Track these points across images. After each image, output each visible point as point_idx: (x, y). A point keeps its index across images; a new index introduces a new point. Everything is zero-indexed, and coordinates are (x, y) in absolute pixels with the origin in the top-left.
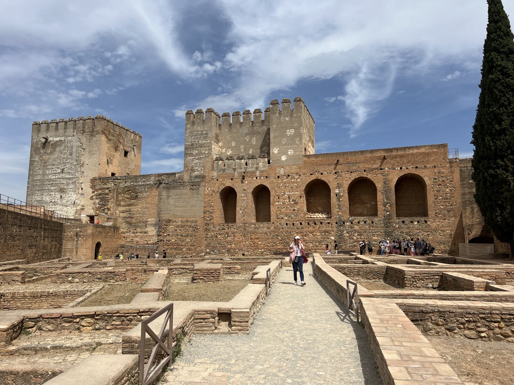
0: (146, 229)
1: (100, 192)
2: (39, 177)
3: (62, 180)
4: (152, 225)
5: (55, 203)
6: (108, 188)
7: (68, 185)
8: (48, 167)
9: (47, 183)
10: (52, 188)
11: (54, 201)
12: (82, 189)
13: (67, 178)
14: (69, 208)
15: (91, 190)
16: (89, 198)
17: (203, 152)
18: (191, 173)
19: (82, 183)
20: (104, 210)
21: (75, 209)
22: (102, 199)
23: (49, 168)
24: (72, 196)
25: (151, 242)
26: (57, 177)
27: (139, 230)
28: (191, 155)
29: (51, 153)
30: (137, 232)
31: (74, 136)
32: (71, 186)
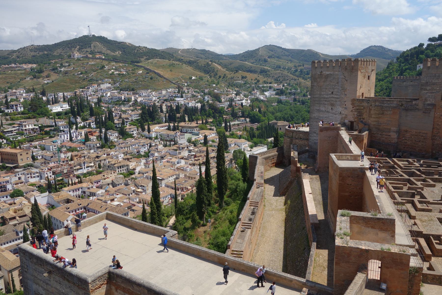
0: (390, 134)
1: (357, 108)
2: (317, 96)
3: (332, 99)
4: (394, 132)
5: (328, 112)
6: (362, 106)
7: (336, 102)
8: (323, 90)
9: (322, 99)
10: (326, 103)
11: (327, 110)
12: (345, 105)
13: (335, 98)
14: (337, 115)
15: (351, 106)
16: (351, 110)
17: (435, 88)
18: (424, 102)
19: (345, 101)
20: (360, 119)
21: (341, 116)
22: (359, 112)
23: (324, 91)
24: (340, 109)
25: (393, 142)
26: (329, 96)
27: (384, 133)
28: (426, 89)
29: (324, 81)
30: (383, 135)
31: (339, 71)
32: (338, 103)
